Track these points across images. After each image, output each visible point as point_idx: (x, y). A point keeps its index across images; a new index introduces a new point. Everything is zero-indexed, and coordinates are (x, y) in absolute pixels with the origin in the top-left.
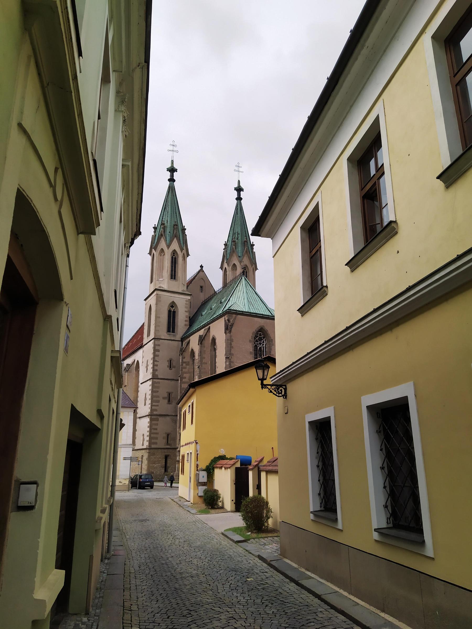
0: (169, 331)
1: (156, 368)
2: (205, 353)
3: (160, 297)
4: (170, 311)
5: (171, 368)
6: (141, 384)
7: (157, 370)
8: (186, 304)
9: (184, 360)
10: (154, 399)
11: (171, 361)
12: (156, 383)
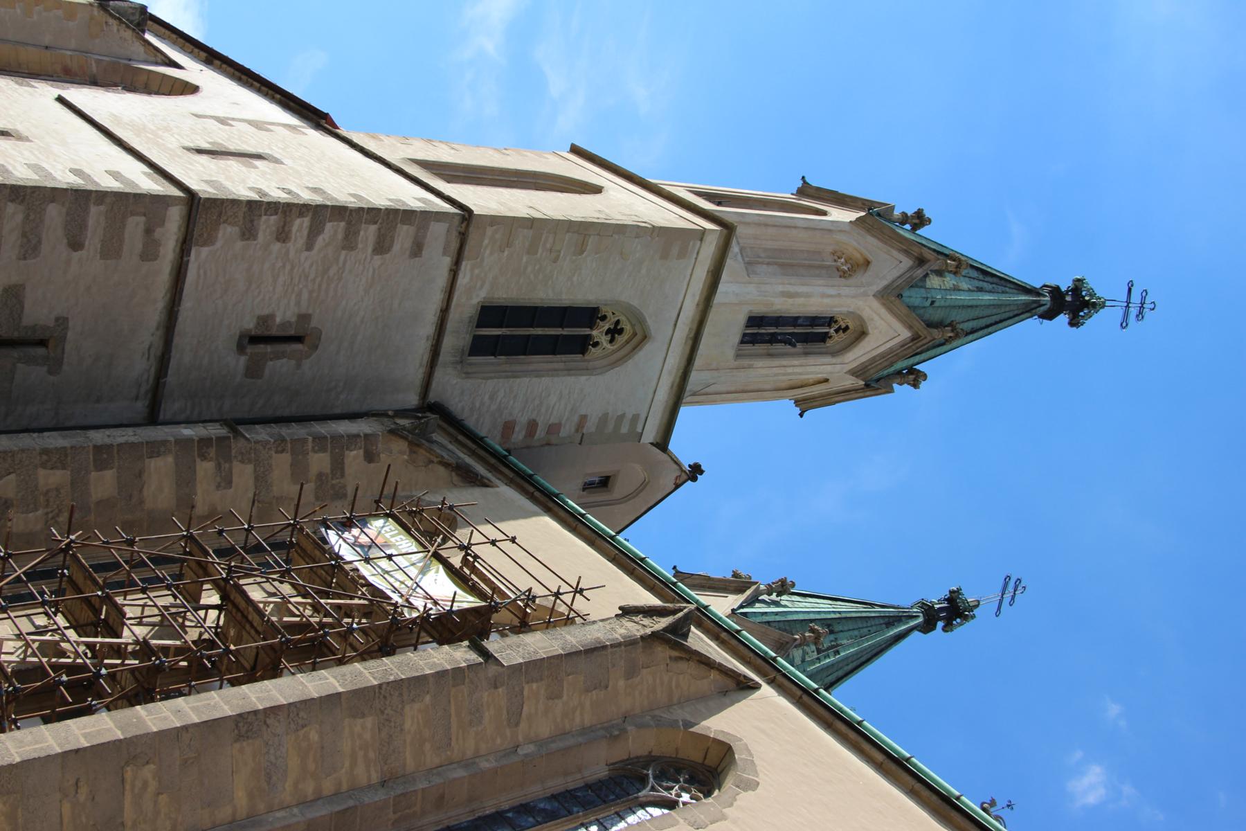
0: (490, 314)
1: (267, 224)
2: (587, 690)
4: (590, 315)
5: (250, 349)
6: (60, 100)
7: (249, 233)
8: (621, 417)
9: (354, 458)
10: (11, 208)
11: (298, 339)
12: (149, 231)
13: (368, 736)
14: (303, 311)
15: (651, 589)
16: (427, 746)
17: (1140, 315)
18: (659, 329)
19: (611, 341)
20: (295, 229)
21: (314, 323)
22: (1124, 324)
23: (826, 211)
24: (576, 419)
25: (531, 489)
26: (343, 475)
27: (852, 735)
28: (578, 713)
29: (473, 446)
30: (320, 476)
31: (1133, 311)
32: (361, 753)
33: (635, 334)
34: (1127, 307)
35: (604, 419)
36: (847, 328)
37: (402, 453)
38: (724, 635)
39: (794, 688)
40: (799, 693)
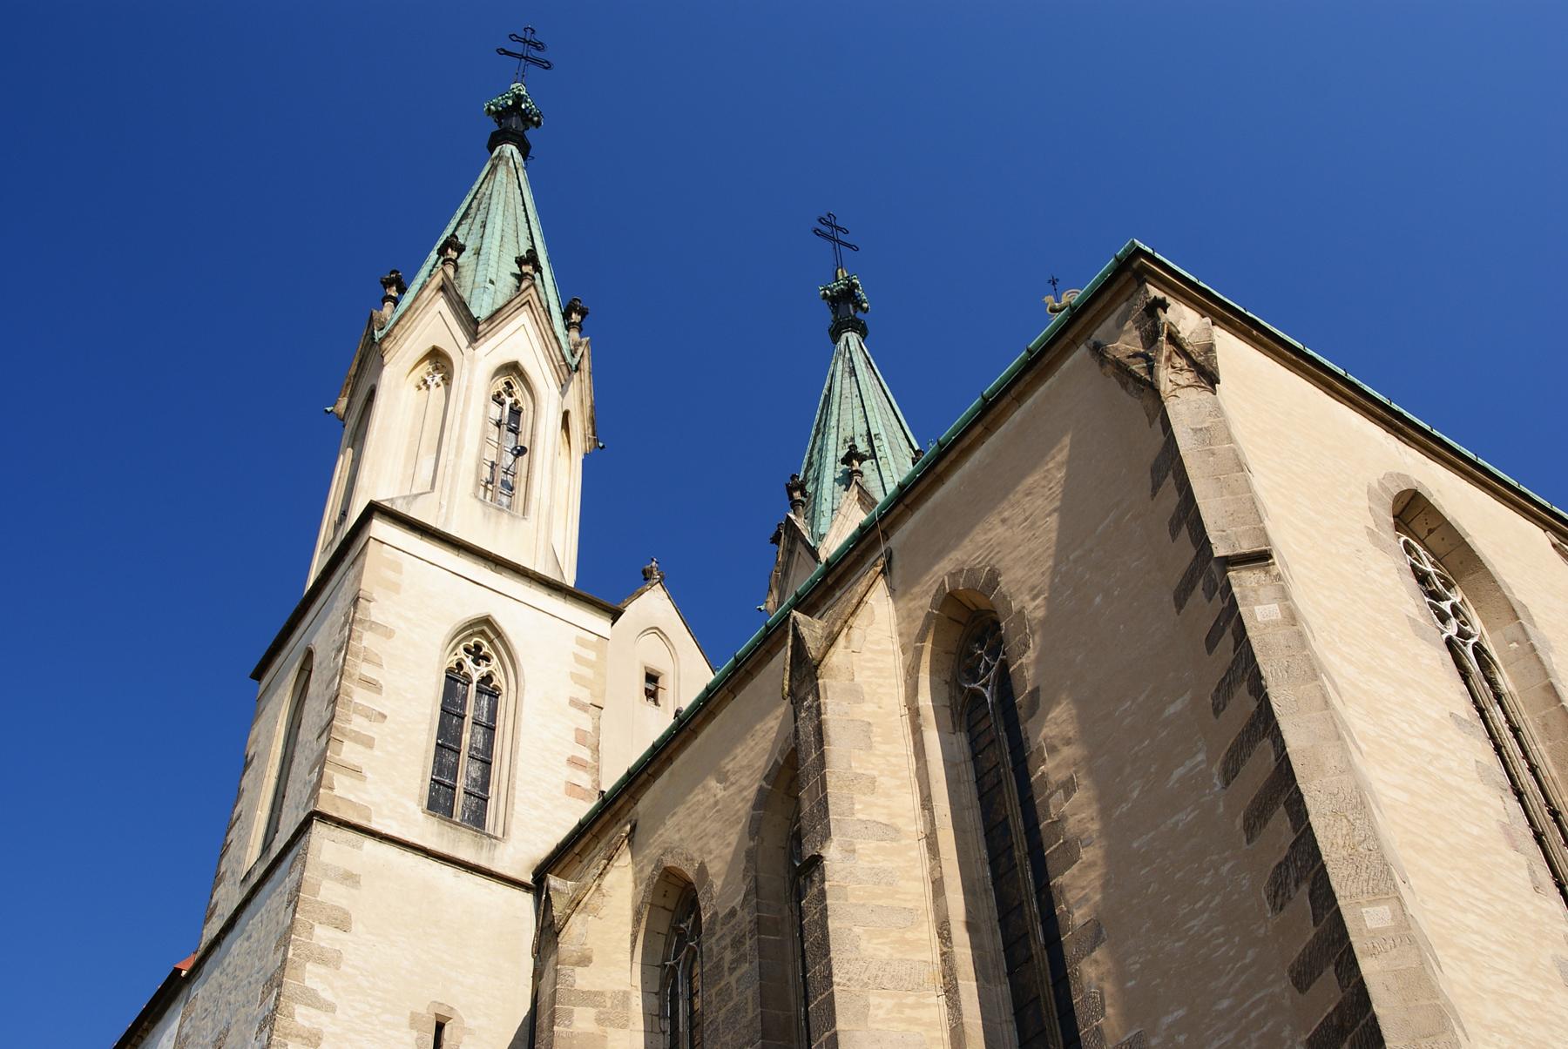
0: (439, 801)
3: (398, 568)
8: (579, 659)
11: (440, 1027)
13: (889, 1003)
14: (406, 1021)
15: (770, 654)
16: (909, 935)
17: (538, 46)
18: (477, 604)
19: (487, 658)
20: (307, 1024)
21: (422, 1010)
22: (546, 65)
23: (371, 387)
24: (574, 711)
25: (644, 776)
26: (602, 994)
27: (953, 455)
28: (894, 760)
29: (589, 836)
30: (600, 1021)
31: (535, 53)
32: (908, 1012)
33: (482, 633)
34: (526, 58)
35: (577, 679)
36: (508, 383)
37: (585, 922)
38: (830, 581)
39: (896, 512)
40: (901, 507)
